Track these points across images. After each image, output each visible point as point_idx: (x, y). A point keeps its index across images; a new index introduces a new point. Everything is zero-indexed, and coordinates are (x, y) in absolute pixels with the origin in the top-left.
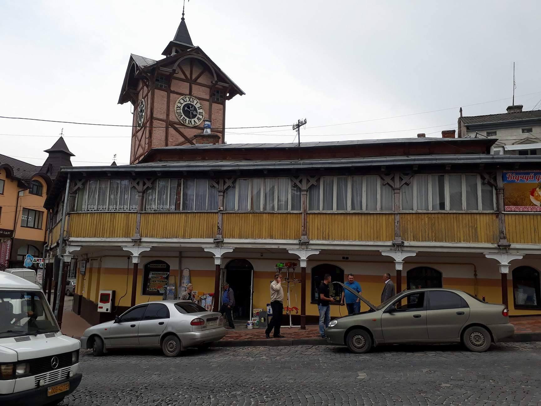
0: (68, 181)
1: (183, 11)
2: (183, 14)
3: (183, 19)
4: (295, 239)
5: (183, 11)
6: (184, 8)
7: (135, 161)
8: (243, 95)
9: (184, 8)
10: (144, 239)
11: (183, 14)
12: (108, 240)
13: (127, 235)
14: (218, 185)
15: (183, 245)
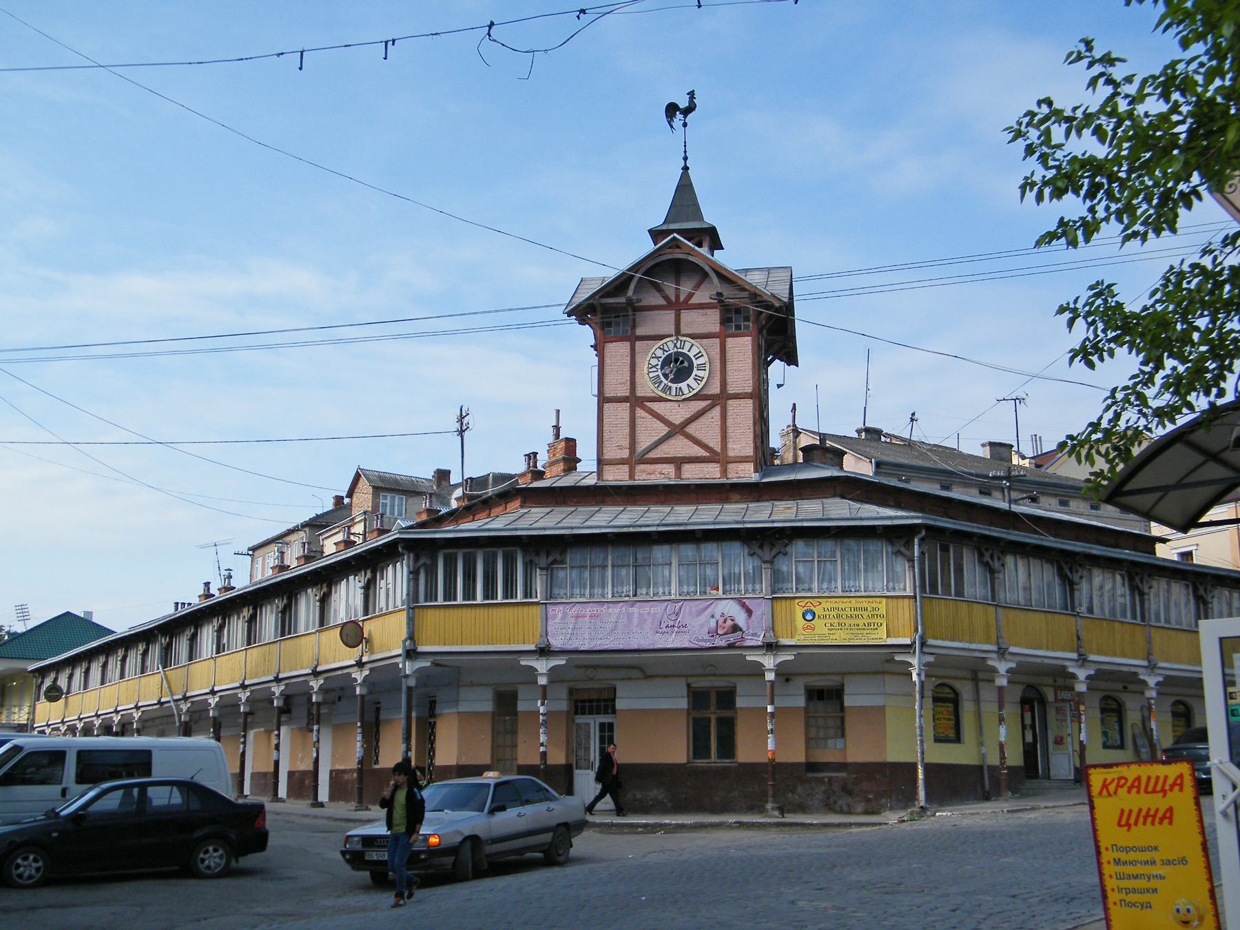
0: (916, 541)
1: (685, 152)
2: (685, 159)
3: (686, 168)
4: (1143, 659)
5: (685, 152)
6: (685, 146)
7: (643, 463)
8: (793, 367)
9: (685, 146)
10: (1013, 649)
11: (685, 159)
12: (973, 646)
13: (988, 642)
14: (1071, 572)
15: (1046, 661)
